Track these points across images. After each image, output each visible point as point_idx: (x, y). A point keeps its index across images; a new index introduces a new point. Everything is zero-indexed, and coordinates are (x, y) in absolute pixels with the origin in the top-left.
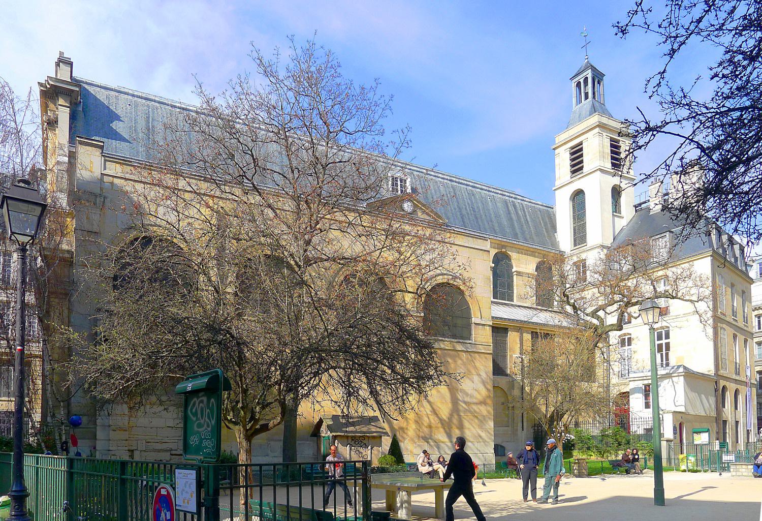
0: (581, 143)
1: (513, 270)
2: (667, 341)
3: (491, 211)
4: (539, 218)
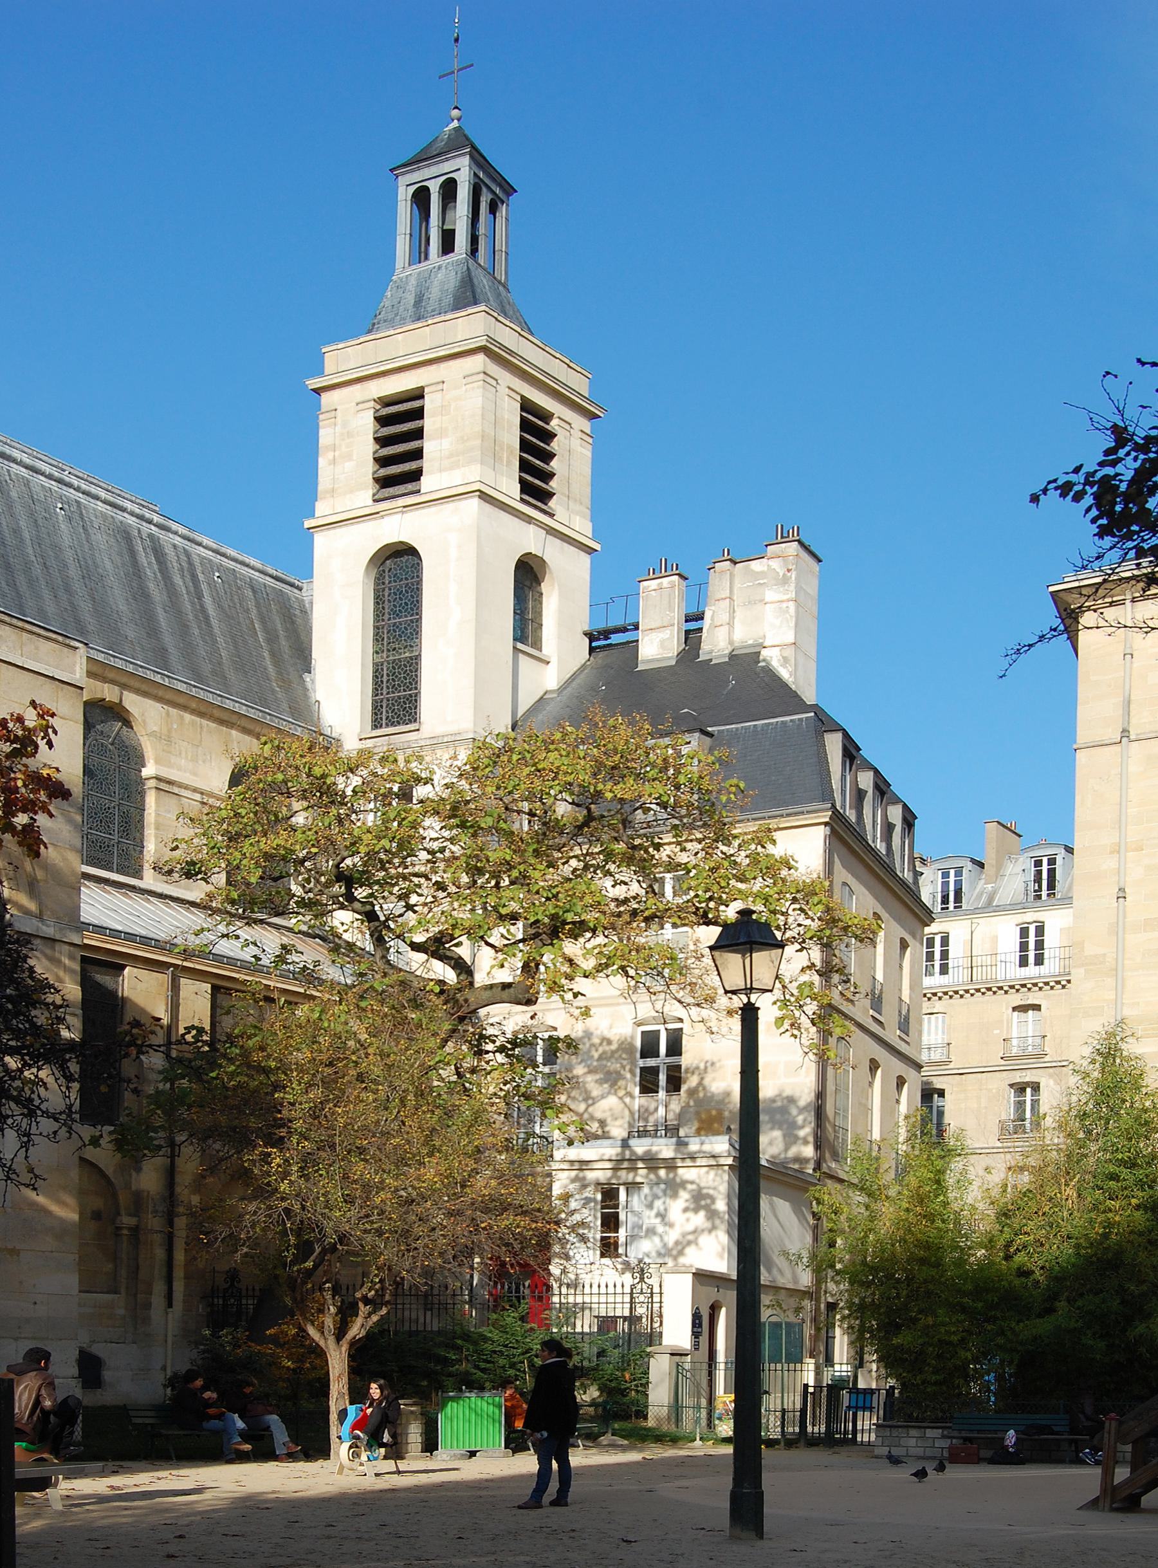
1: (146, 772)
3: (69, 555)
4: (247, 611)
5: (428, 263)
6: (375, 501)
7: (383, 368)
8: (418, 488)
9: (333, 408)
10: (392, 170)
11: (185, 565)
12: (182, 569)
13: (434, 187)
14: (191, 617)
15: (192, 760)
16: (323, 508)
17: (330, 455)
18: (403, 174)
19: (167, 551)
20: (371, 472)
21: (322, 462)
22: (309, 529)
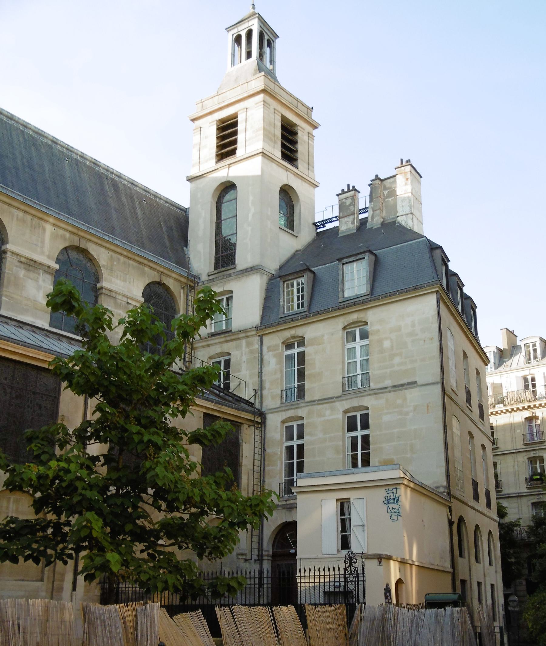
0: (235, 116)
2: (365, 432)
10: (226, 29)
15: (123, 281)
18: (230, 30)
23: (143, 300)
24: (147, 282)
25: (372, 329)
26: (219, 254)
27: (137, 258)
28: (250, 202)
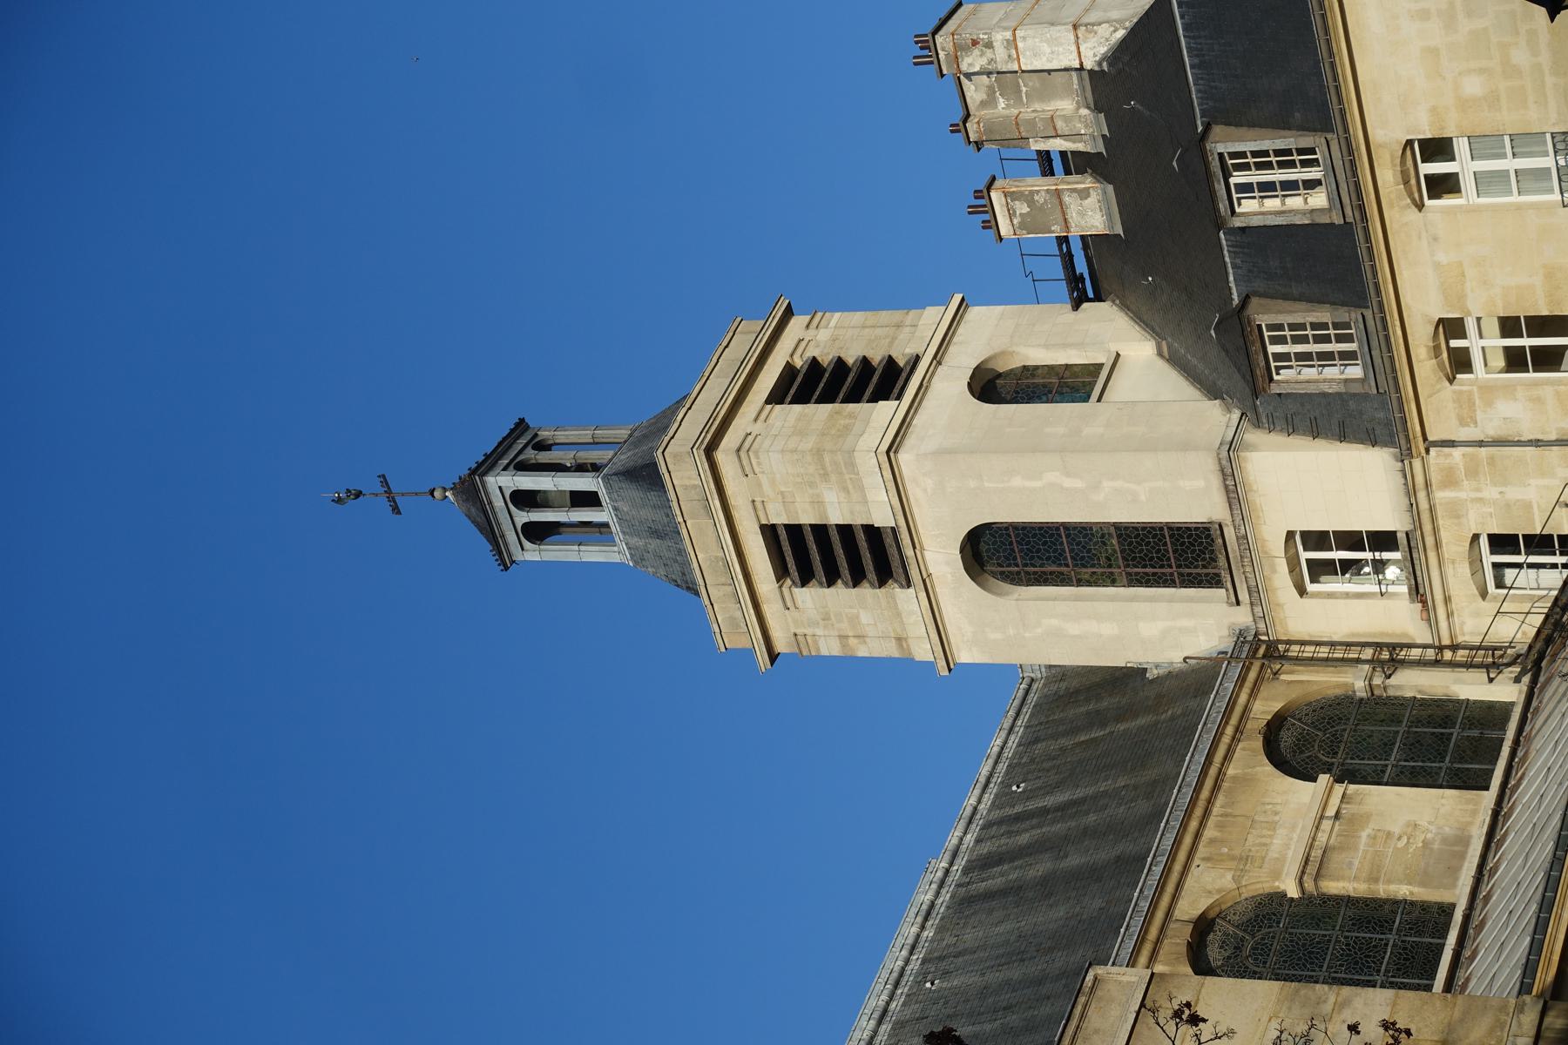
0: (770, 532)
1: (1293, 892)
3: (994, 977)
4: (1063, 750)
5: (611, 524)
6: (909, 585)
7: (740, 577)
8: (889, 531)
9: (793, 639)
11: (1004, 829)
12: (1009, 833)
13: (523, 517)
14: (1073, 824)
15: (1274, 829)
16: (924, 651)
17: (852, 642)
18: (510, 555)
19: (985, 851)
20: (871, 590)
21: (862, 652)
22: (950, 670)
23: (1324, 779)
24: (1270, 768)
25: (1427, 128)
26: (1172, 574)
27: (1205, 794)
28: (1029, 484)
